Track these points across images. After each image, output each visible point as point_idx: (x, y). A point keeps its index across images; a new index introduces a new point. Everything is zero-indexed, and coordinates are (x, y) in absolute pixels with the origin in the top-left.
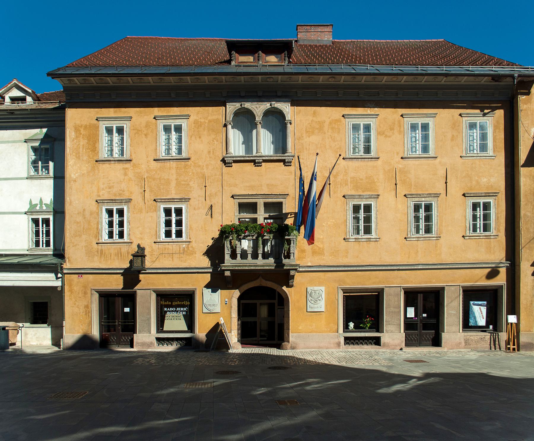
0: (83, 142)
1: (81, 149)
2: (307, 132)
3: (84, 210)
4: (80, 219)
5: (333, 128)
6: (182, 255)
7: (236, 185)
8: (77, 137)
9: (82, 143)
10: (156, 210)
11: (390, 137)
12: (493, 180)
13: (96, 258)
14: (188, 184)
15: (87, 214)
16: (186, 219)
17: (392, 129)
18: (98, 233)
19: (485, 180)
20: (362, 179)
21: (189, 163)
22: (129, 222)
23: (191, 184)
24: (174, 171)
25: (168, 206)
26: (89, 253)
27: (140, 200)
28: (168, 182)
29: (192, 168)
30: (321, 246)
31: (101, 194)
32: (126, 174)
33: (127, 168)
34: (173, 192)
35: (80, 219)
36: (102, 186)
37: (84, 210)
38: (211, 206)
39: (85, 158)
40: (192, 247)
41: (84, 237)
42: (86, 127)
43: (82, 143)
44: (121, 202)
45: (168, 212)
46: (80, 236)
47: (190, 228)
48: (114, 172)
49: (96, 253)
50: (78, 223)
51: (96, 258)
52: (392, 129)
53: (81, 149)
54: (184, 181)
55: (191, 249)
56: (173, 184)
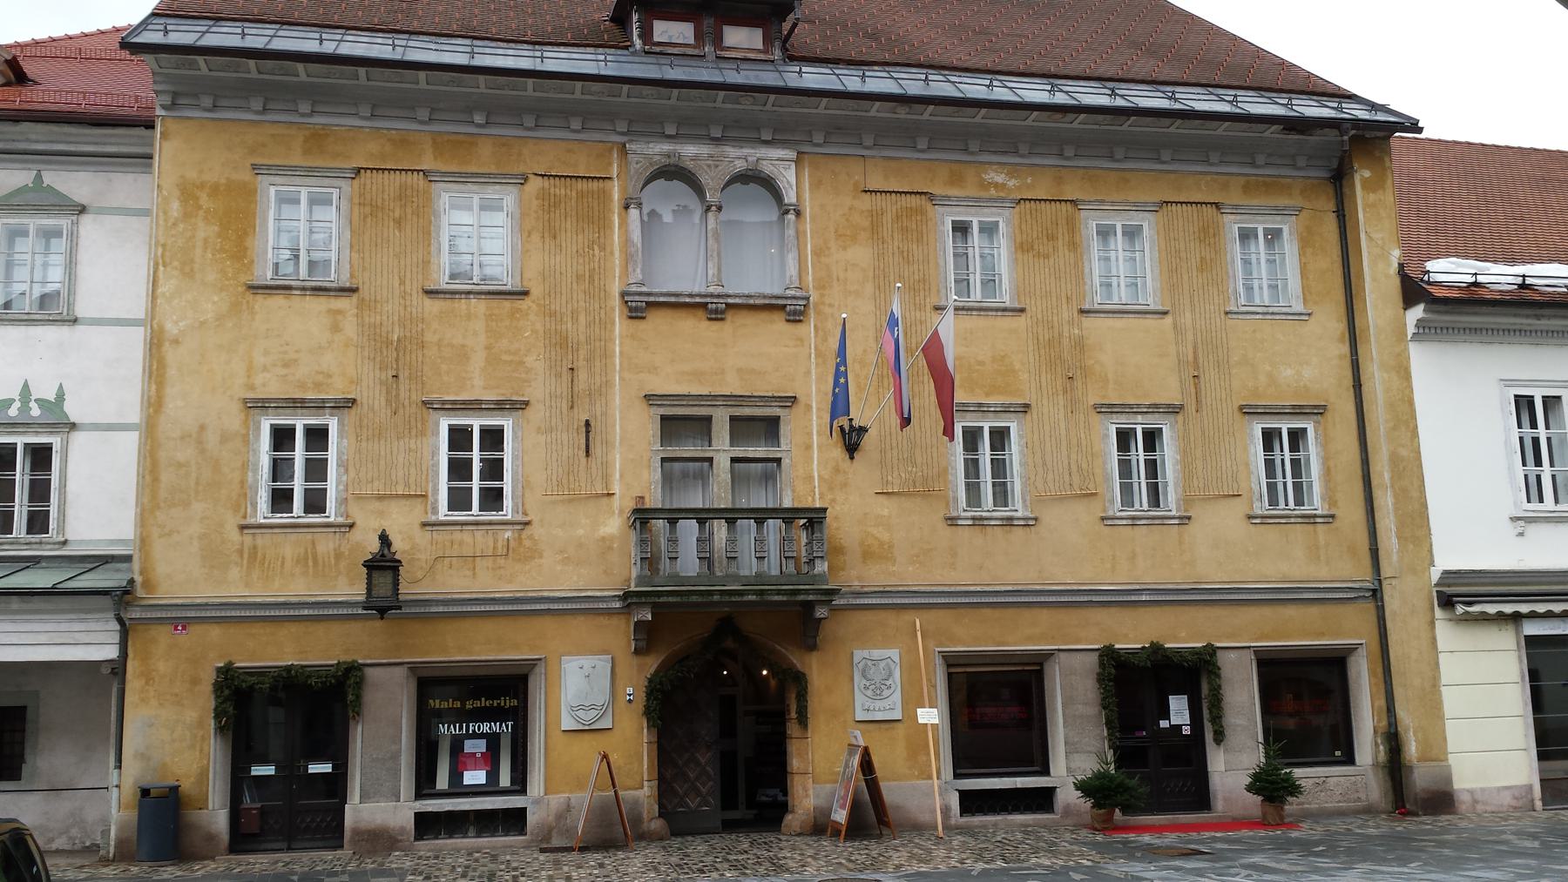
0: (205, 231)
1: (198, 251)
2: (839, 236)
3: (202, 428)
4: (186, 453)
5: (905, 230)
6: (501, 561)
7: (653, 370)
8: (187, 216)
9: (201, 234)
10: (429, 431)
11: (1047, 257)
12: (1307, 373)
13: (234, 573)
14: (522, 363)
15: (212, 439)
16: (515, 458)
17: (1052, 238)
18: (245, 495)
19: (1289, 372)
20: (982, 363)
21: (525, 304)
22: (343, 465)
23: (530, 360)
24: (479, 325)
25: (460, 421)
26: (213, 556)
27: (379, 402)
28: (463, 355)
29: (532, 317)
30: (885, 536)
31: (258, 380)
32: (336, 328)
33: (339, 312)
34: (478, 382)
35: (186, 453)
36: (259, 359)
37: (202, 428)
38: (587, 424)
39: (211, 277)
40: (531, 537)
41: (198, 507)
42: (215, 190)
43: (201, 234)
44: (319, 406)
45: (459, 438)
46: (186, 504)
47: (523, 485)
48: (305, 322)
49: (235, 557)
50: (180, 465)
51: (234, 573)
52: (1052, 238)
53: (198, 251)
54: (508, 352)
55: (527, 543)
56: (478, 360)
